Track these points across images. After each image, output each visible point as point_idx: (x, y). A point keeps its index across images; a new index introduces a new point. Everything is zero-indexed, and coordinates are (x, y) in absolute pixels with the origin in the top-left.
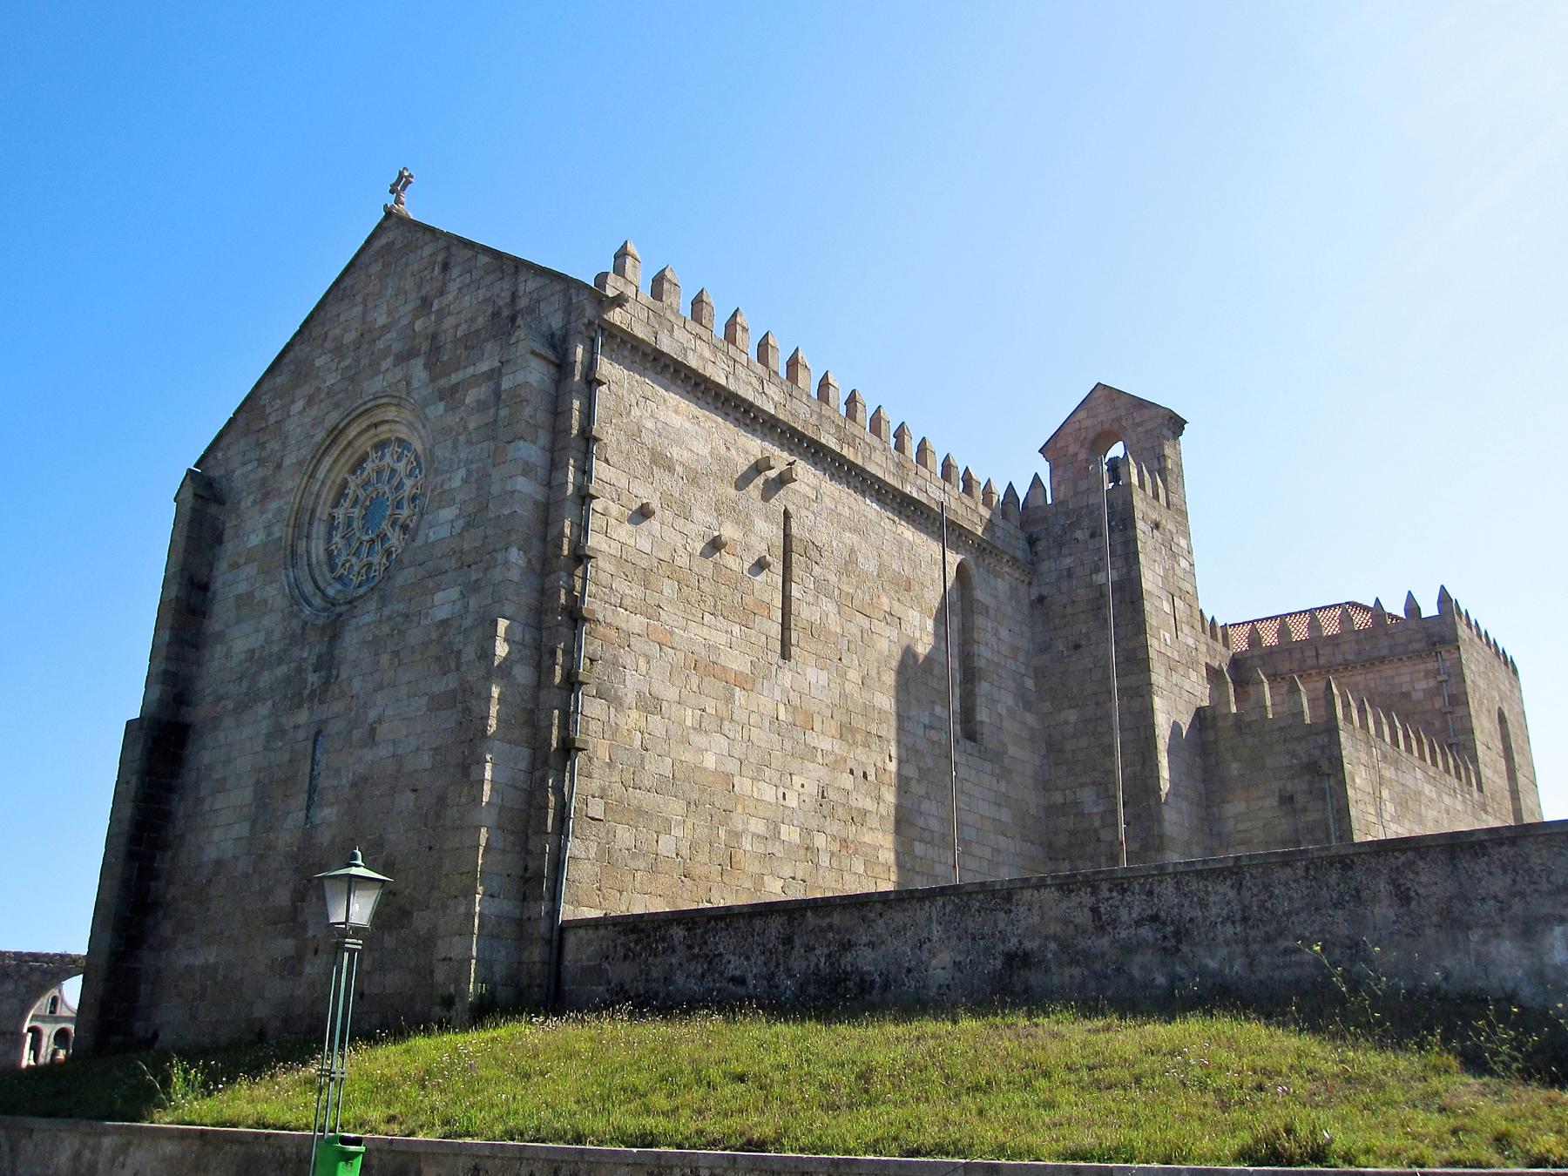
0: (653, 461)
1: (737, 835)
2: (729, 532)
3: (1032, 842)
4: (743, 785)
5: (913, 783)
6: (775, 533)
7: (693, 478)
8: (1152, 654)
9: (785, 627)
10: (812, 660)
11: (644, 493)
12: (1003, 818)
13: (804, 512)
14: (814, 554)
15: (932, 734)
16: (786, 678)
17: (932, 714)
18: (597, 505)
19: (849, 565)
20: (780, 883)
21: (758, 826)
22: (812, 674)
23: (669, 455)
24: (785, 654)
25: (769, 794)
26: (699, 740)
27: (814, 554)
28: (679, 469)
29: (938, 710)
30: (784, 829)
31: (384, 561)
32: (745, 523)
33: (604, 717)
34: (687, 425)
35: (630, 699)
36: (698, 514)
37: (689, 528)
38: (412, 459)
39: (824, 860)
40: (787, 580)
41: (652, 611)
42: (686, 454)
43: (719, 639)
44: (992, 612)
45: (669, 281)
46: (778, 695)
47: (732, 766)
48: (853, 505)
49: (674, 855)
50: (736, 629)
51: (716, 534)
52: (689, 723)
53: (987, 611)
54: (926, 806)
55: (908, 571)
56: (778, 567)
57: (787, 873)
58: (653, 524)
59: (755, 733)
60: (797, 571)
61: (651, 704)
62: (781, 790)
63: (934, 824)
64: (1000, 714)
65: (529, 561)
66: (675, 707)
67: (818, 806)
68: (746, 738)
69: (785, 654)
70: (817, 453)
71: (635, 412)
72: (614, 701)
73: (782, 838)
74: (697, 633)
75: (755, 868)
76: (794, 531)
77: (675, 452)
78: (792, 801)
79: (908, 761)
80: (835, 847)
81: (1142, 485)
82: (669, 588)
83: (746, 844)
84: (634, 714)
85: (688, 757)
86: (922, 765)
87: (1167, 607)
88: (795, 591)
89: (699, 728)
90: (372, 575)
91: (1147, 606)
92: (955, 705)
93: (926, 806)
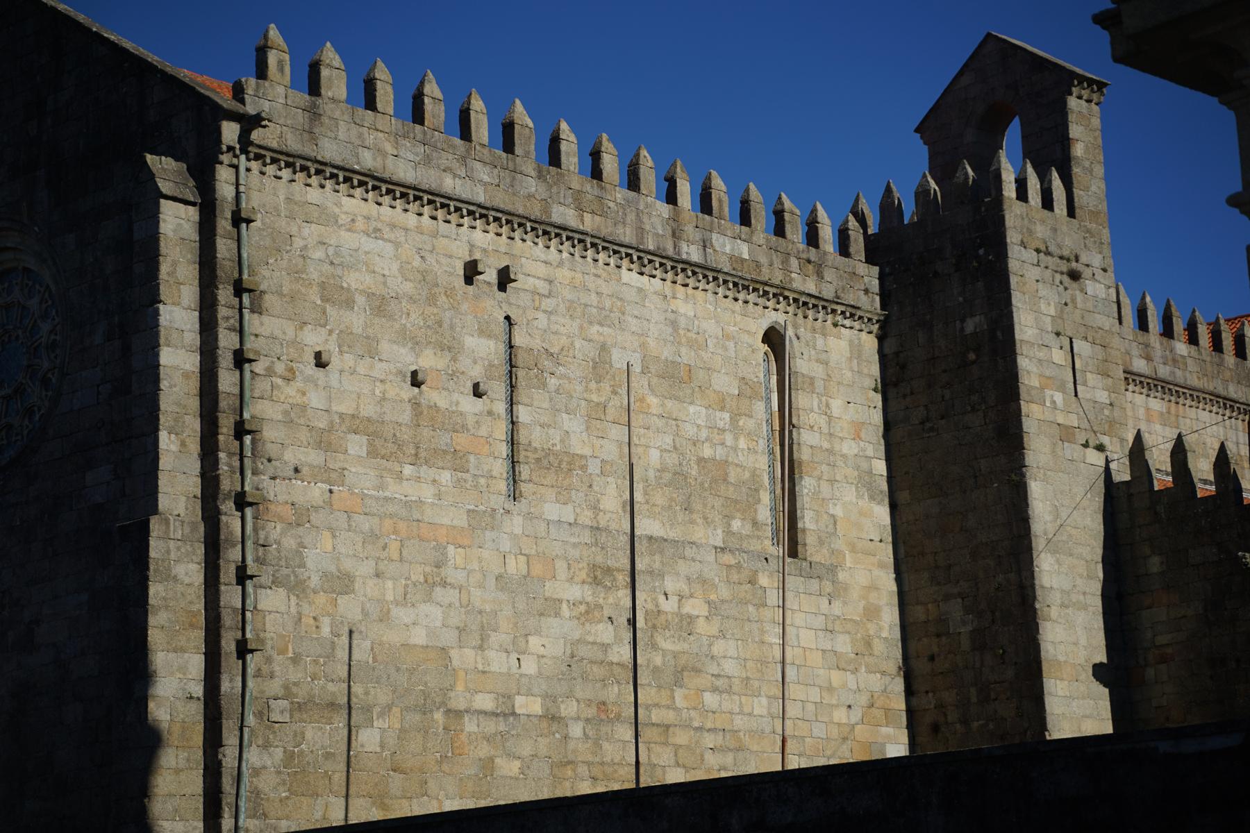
0: (325, 299)
1: (458, 714)
2: (428, 361)
3: (883, 673)
4: (464, 658)
5: (701, 621)
6: (492, 349)
7: (380, 305)
8: (1029, 425)
9: (513, 461)
10: (550, 494)
11: (314, 339)
12: (839, 649)
13: (531, 314)
14: (547, 364)
15: (728, 559)
16: (516, 524)
17: (728, 532)
18: (259, 367)
19: (599, 366)
20: (517, 764)
21: (485, 702)
22: (552, 510)
23: (345, 285)
24: (515, 496)
25: (498, 662)
26: (402, 615)
27: (547, 364)
28: (360, 300)
29: (736, 525)
30: (519, 701)
31: (26, 422)
32: (451, 348)
33: (283, 609)
34: (364, 239)
35: (315, 581)
36: (385, 347)
37: (380, 369)
38: (47, 295)
39: (576, 730)
40: (511, 403)
41: (332, 477)
42: (368, 280)
43: (428, 493)
44: (819, 385)
45: (330, 66)
46: (506, 545)
47: (448, 638)
48: (605, 289)
49: (378, 750)
50: (446, 477)
51: (413, 368)
52: (389, 597)
53: (812, 384)
54: (719, 648)
55: (687, 356)
56: (498, 390)
57: (526, 749)
58: (331, 376)
59: (477, 596)
60: (522, 394)
61: (342, 583)
62: (514, 656)
63: (730, 667)
64: (833, 516)
65: (183, 444)
66: (371, 583)
67: (565, 669)
68: (465, 602)
69: (515, 496)
70: (546, 230)
71: (298, 243)
72: (298, 588)
73: (518, 711)
74: (394, 489)
75: (484, 750)
76: (518, 340)
77: (353, 280)
78: (530, 667)
79: (691, 596)
80: (591, 712)
81: (1022, 195)
82: (356, 445)
83: (470, 725)
84: (321, 599)
85: (392, 637)
86: (713, 597)
87: (1059, 357)
88: (523, 414)
89: (404, 600)
90: (14, 439)
91: (1023, 362)
92: (764, 514)
93: (719, 648)
